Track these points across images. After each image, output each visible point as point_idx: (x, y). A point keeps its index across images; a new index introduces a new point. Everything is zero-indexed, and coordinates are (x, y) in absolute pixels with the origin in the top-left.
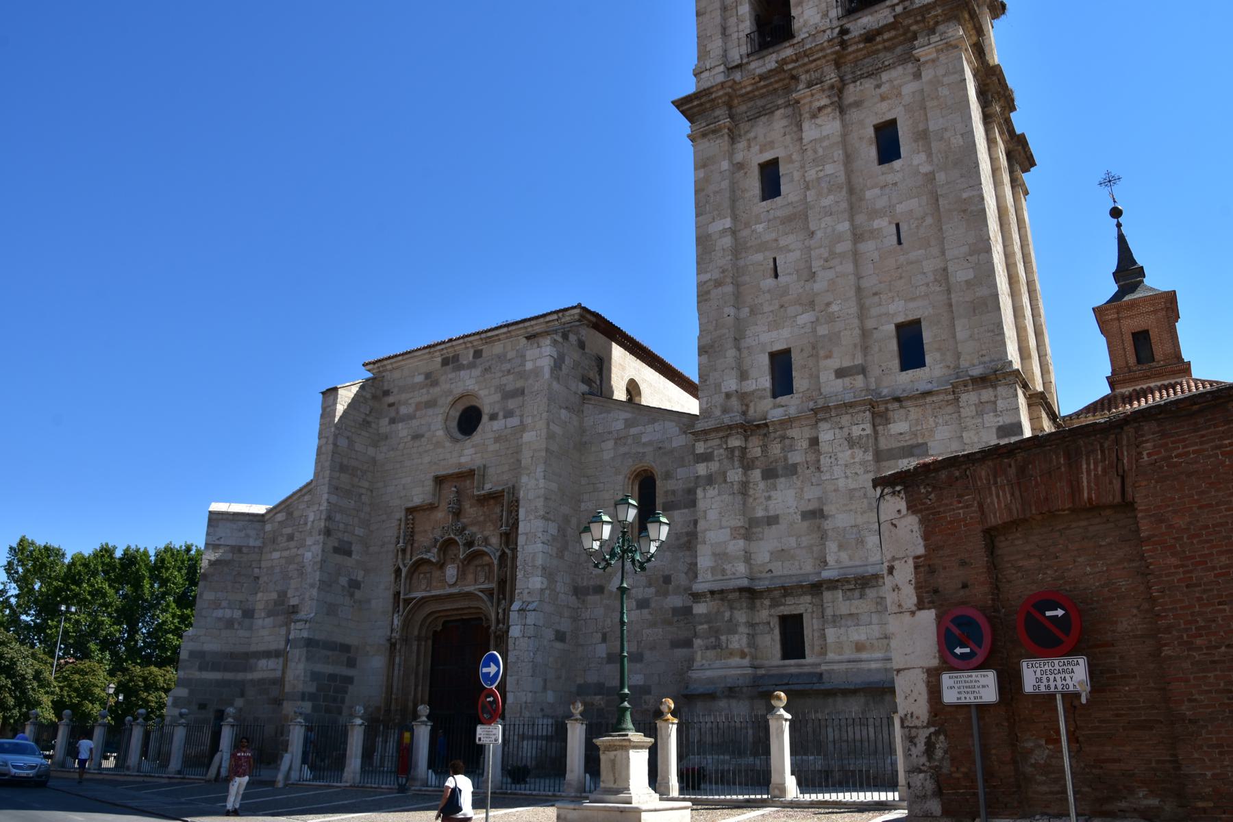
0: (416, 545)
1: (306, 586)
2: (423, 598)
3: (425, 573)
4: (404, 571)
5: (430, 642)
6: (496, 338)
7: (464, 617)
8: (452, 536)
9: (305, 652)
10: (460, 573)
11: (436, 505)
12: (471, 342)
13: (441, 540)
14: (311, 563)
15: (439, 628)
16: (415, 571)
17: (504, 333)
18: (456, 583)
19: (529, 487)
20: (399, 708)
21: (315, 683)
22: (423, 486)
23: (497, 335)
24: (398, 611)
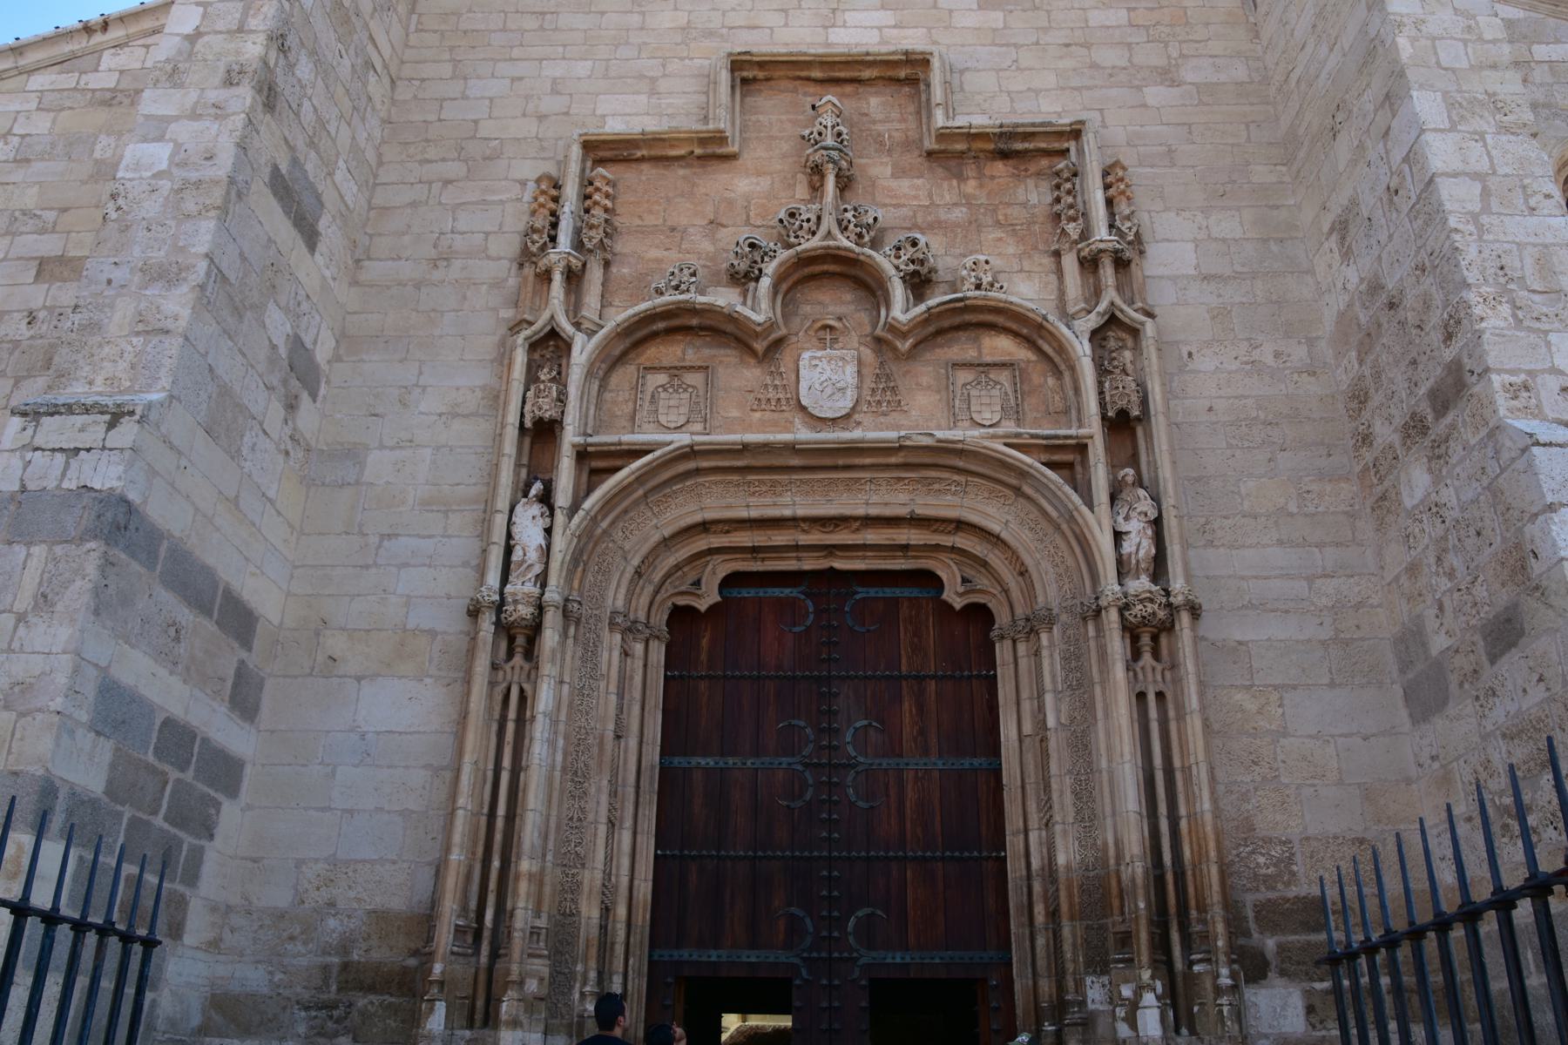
0: (621, 271)
1: (118, 275)
2: (691, 452)
3: (675, 371)
4: (582, 351)
5: (658, 653)
7: (839, 565)
8: (846, 243)
9: (91, 569)
10: (869, 383)
11: (733, 148)
13: (784, 255)
14: (165, 185)
15: (708, 598)
16: (621, 359)
18: (847, 416)
19: (1432, 28)
20: (542, 923)
21: (105, 750)
22: (653, 92)
24: (546, 499)
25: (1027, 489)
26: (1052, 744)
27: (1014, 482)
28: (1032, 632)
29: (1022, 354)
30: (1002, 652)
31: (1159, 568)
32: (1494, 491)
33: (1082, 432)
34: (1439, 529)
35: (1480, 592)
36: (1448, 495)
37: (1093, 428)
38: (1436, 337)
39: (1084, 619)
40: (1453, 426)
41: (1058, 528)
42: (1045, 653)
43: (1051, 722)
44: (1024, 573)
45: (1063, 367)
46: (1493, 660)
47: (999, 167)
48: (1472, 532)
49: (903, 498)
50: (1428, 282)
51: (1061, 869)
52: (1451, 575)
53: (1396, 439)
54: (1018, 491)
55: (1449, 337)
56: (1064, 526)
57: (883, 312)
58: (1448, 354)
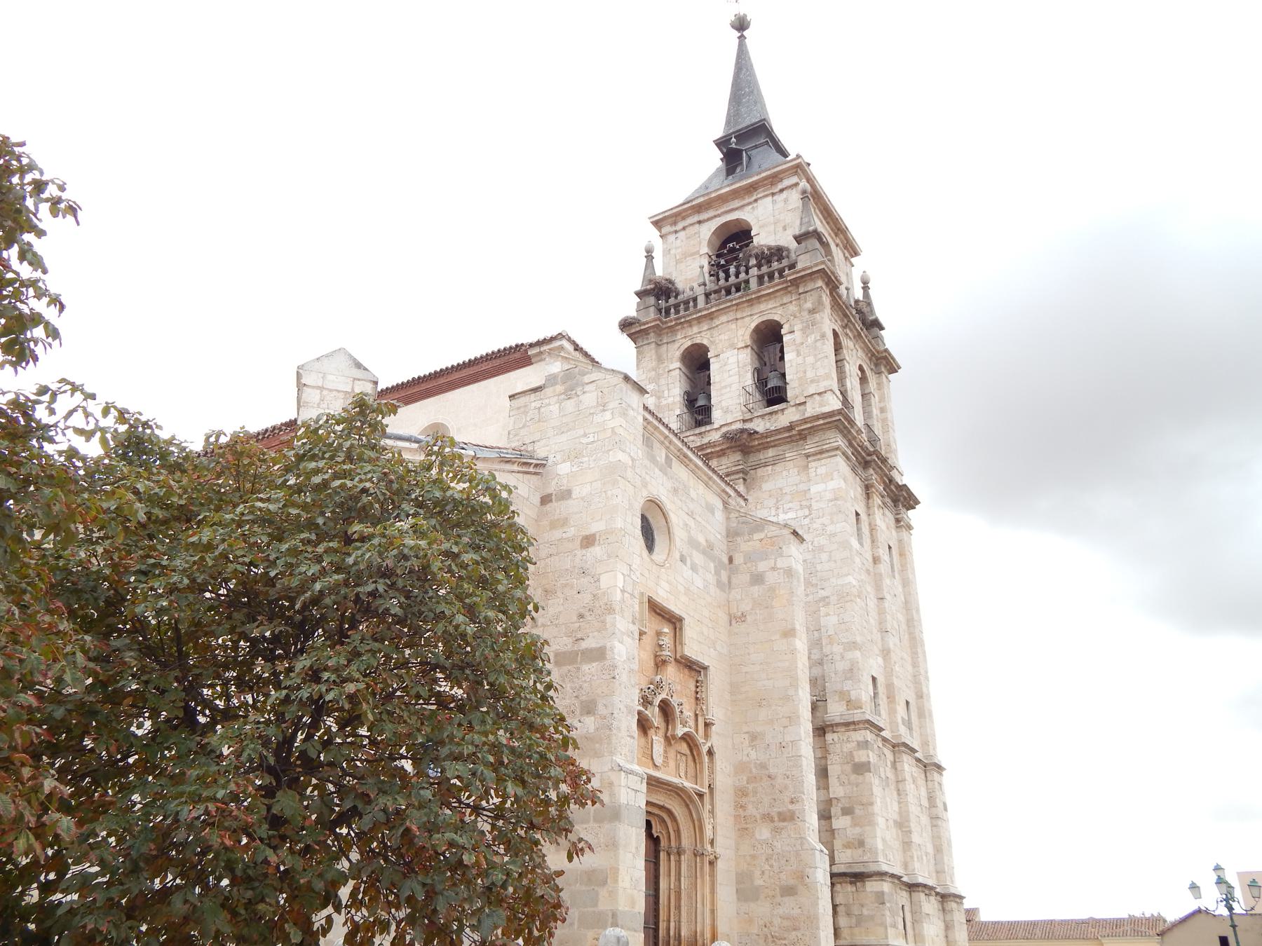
6: (688, 463)
12: (670, 442)
17: (696, 465)
23: (691, 460)
25: (691, 807)
26: (683, 895)
27: (688, 802)
28: (679, 854)
29: (688, 752)
30: (663, 855)
31: (712, 842)
32: (797, 854)
33: (704, 790)
34: (770, 851)
35: (783, 876)
36: (778, 845)
37: (706, 790)
38: (787, 800)
39: (695, 855)
40: (786, 827)
41: (693, 821)
42: (683, 863)
43: (683, 888)
44: (678, 832)
45: (697, 761)
46: (782, 896)
47: (686, 671)
48: (785, 859)
49: (663, 799)
50: (788, 782)
51: (683, 938)
52: (771, 866)
53: (758, 816)
54: (687, 806)
55: (792, 802)
56: (696, 822)
57: (670, 727)
58: (791, 807)
